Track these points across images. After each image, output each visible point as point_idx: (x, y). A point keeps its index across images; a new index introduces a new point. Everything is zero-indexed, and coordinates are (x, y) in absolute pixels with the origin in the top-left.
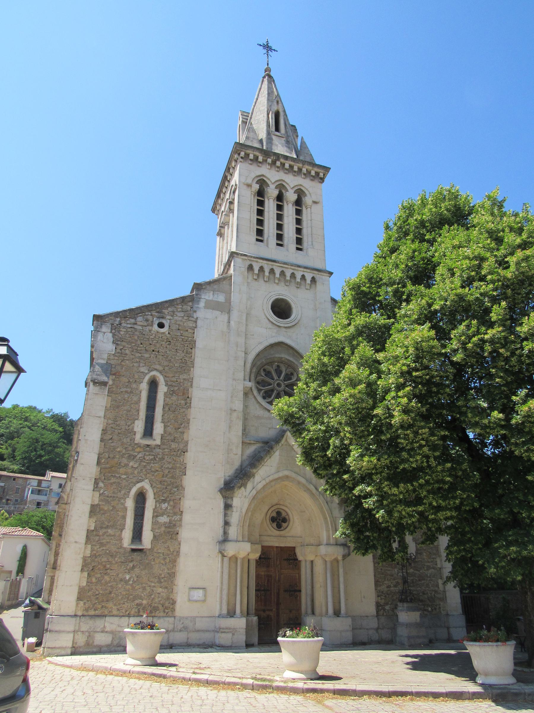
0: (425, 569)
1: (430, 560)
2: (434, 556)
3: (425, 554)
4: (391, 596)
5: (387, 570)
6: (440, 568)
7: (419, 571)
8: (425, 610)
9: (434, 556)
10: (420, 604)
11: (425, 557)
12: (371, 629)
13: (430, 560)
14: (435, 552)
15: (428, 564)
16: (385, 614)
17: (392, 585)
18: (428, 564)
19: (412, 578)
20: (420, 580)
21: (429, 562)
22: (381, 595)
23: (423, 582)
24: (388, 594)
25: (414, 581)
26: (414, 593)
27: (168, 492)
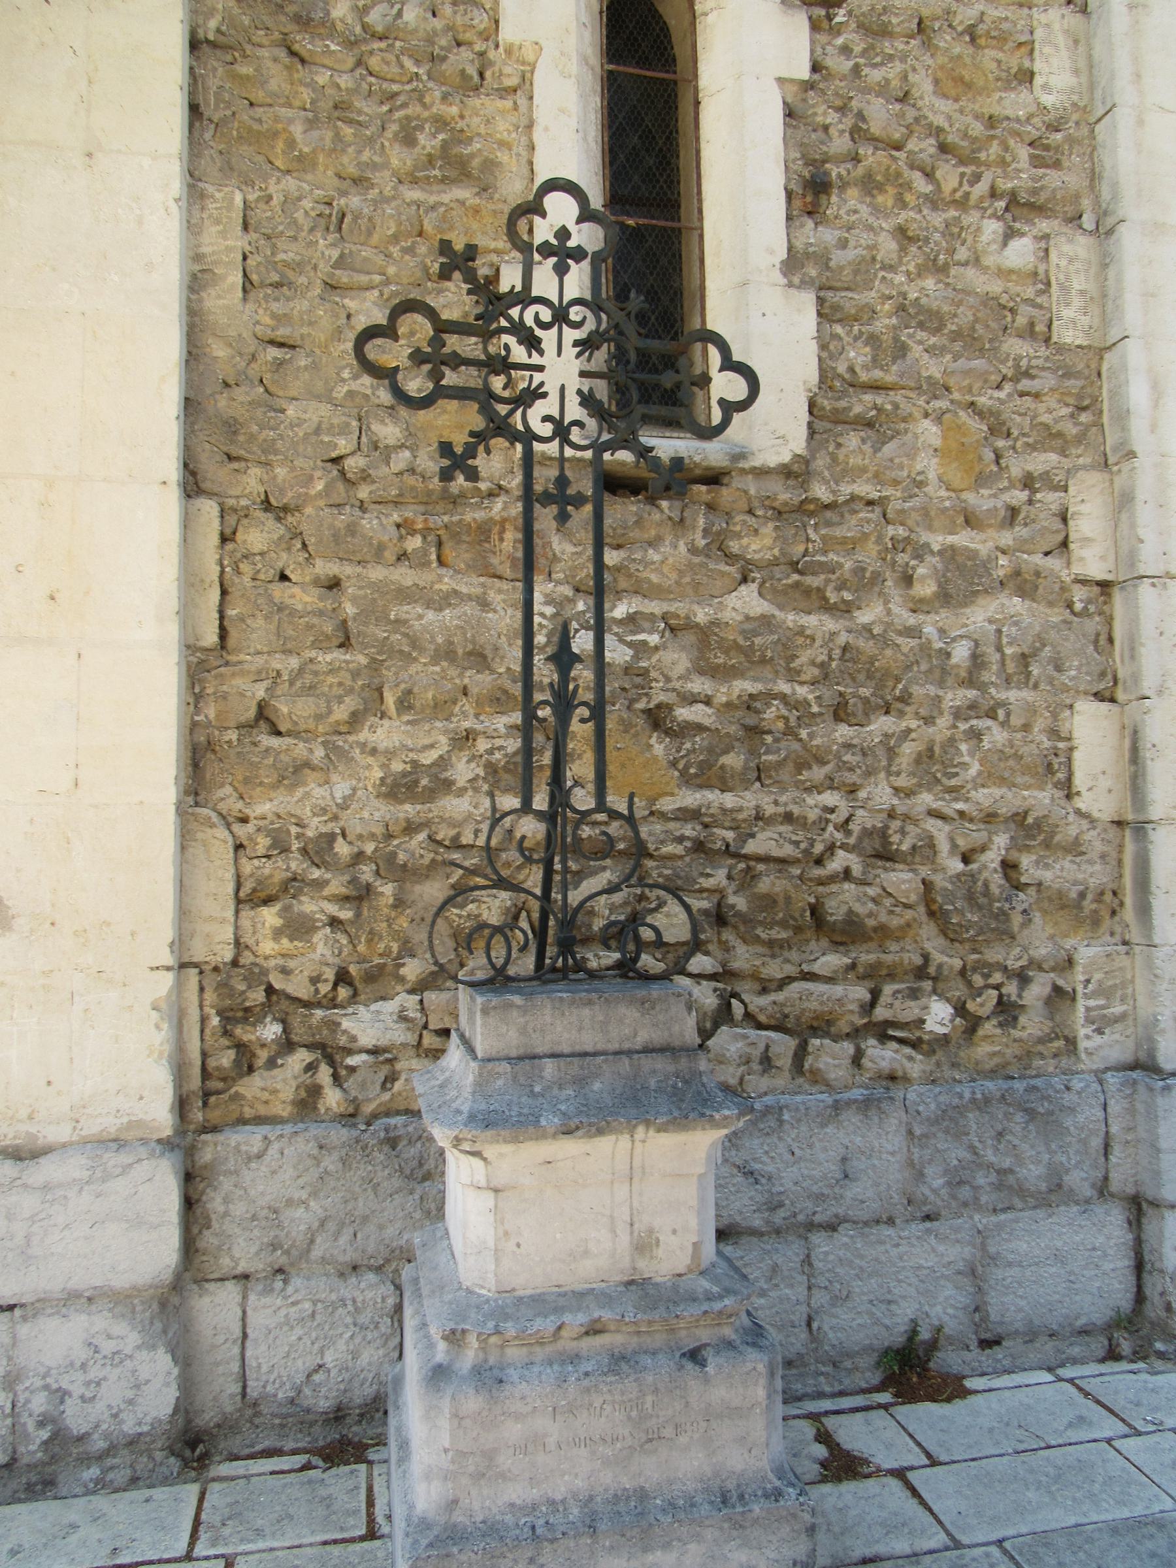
0: (926, 588)
1: (981, 501)
2: (1043, 461)
3: (929, 432)
4: (433, 891)
5: (404, 595)
6: (1105, 586)
7: (845, 609)
8: (883, 1032)
9: (1043, 461)
10: (831, 961)
11: (928, 465)
12: (88, 1299)
13: (981, 501)
14: (1052, 412)
15: (963, 539)
16: (332, 1098)
17: (463, 771)
18: (963, 539)
19: (744, 686)
20: (840, 712)
21: (970, 520)
22: (293, 885)
23: (882, 724)
24: (390, 867)
25: (771, 713)
26: (762, 843)
27: (324, 179)
